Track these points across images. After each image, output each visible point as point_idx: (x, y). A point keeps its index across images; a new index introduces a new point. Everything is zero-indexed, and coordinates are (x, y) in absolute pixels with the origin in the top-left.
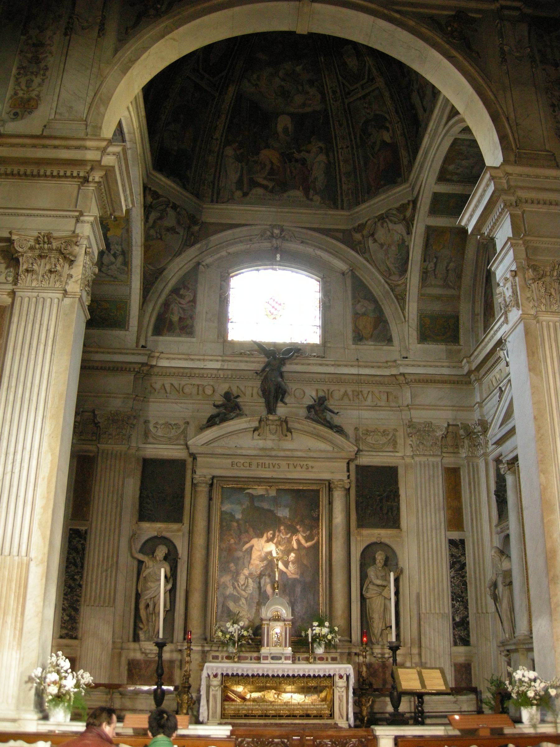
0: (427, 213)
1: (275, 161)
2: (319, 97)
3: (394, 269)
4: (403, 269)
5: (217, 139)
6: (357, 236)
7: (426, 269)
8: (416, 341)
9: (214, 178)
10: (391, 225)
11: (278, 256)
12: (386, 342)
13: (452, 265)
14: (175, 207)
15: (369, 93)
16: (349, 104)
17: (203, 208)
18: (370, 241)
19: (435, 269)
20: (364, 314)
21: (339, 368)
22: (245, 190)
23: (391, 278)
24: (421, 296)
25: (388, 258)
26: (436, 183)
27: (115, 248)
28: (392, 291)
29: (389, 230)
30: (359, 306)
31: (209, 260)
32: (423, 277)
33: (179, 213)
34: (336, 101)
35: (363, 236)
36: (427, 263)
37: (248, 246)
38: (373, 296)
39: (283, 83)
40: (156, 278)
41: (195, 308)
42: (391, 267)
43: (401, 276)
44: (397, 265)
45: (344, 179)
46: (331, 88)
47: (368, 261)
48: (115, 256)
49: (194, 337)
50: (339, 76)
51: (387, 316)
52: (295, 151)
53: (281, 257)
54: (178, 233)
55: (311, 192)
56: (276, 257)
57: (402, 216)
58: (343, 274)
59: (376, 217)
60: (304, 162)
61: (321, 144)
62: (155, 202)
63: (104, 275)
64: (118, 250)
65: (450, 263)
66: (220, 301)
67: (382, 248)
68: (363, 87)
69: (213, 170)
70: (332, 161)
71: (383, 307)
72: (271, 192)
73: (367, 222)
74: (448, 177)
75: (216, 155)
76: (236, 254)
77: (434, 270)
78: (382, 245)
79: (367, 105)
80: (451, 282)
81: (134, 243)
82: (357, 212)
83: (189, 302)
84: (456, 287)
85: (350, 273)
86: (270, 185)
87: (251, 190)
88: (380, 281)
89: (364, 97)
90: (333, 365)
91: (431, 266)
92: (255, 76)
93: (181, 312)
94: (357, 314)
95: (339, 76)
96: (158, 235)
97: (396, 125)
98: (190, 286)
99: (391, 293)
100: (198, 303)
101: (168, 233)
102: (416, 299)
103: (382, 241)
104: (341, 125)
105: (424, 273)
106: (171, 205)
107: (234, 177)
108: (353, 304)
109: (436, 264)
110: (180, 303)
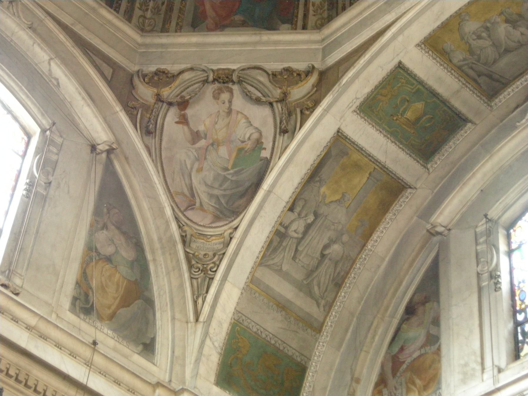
0: (358, 103)
3: (205, 198)
8: (213, 378)
12: (140, 348)
13: (336, 248)
18: (172, 115)
19: (302, 238)
20: (108, 259)
21: (41, 343)
23: (189, 213)
24: (252, 281)
25: (200, 170)
26: (418, 45)
28: (184, 242)
29: (229, 112)
30: (102, 236)
32: (271, 242)
35: (159, 98)
36: (292, 216)
43: (217, 218)
44: (216, 192)
57: (277, 93)
58: (93, 148)
59: (213, 70)
65: (335, 242)
67: (194, 142)
73: (181, 72)
74: (448, 45)
77: (299, 241)
78: (196, 136)
80: (319, 285)
84: (323, 302)
88: (161, 210)
90: (29, 328)
91: (298, 226)
99: (180, 247)
102: (242, 285)
103: (201, 128)
105: (277, 233)
109: (308, 227)
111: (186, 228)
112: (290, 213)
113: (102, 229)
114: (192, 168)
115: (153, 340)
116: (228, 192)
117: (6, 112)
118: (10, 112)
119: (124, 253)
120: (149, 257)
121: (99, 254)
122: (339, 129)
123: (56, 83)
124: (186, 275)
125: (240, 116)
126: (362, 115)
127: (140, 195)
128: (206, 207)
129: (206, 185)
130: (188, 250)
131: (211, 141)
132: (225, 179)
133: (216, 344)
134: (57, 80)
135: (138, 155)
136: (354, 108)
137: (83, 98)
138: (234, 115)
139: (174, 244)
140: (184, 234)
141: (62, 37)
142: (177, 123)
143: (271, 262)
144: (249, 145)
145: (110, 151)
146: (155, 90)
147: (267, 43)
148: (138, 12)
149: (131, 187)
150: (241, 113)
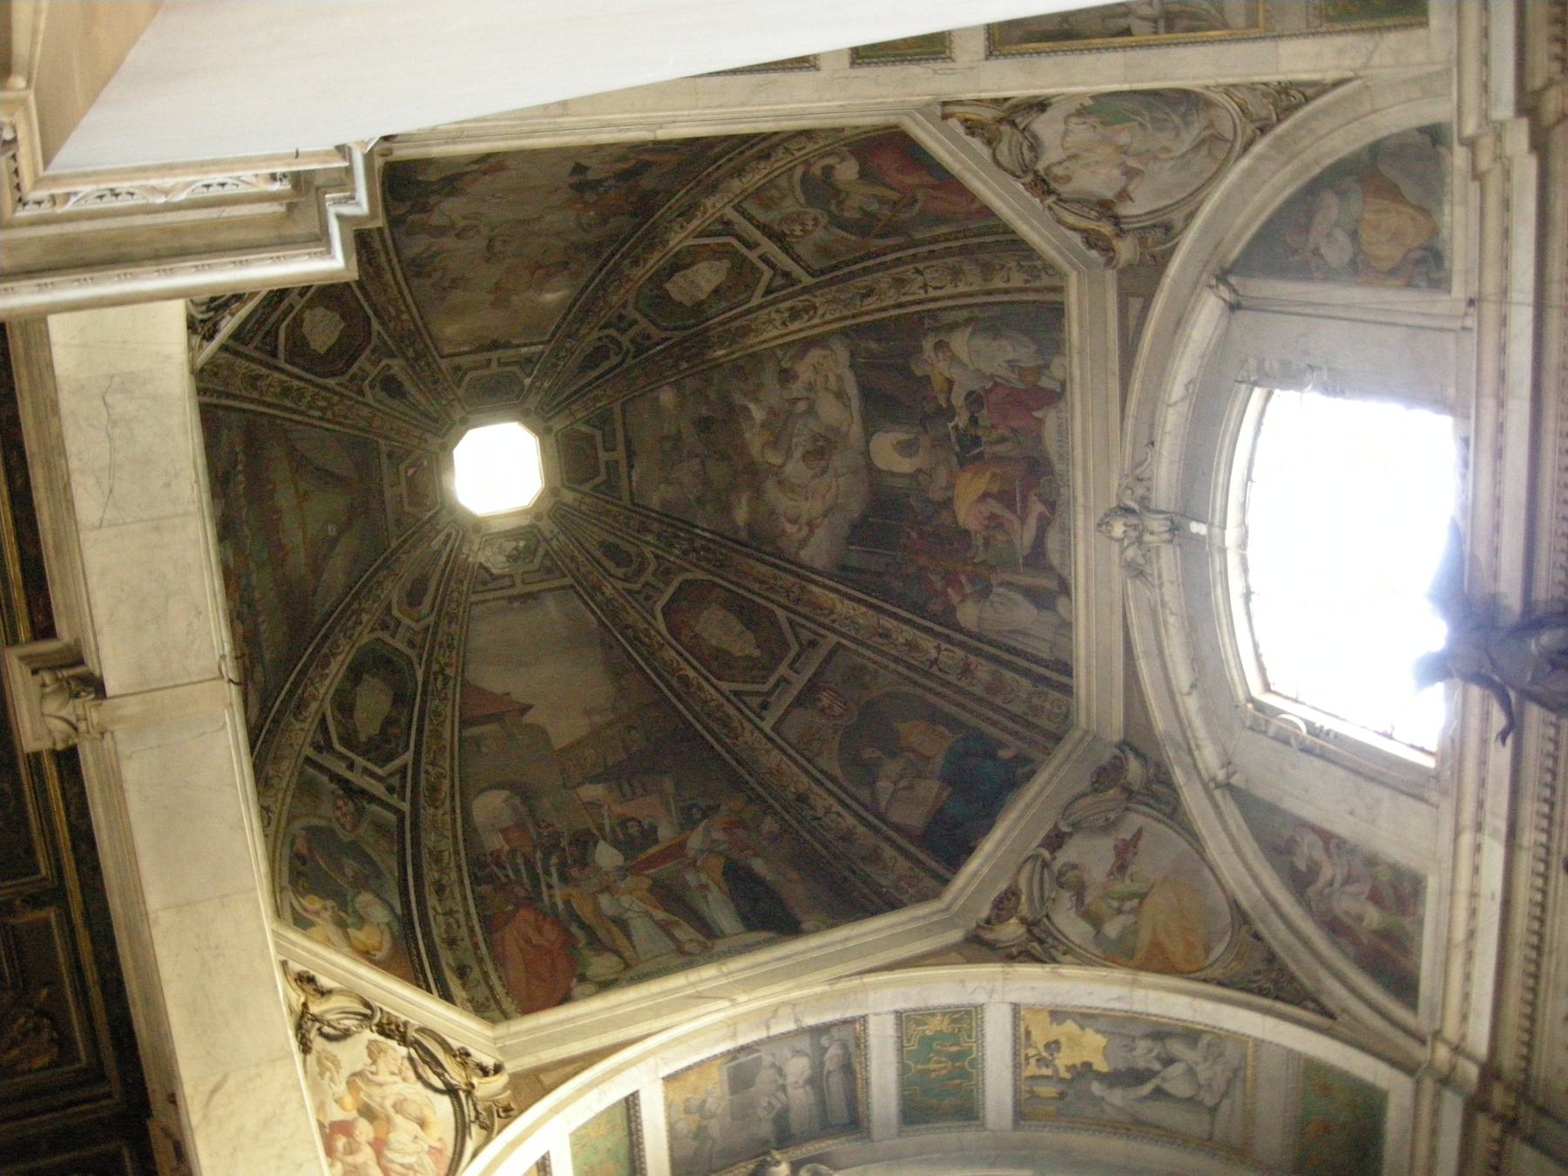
0: (939, 65)
1: (981, 484)
2: (815, 355)
4: (1184, 101)
5: (938, 648)
6: (1126, 249)
7: (1155, 21)
9: (1026, 673)
10: (1052, 155)
11: (1197, 528)
12: (1442, 150)
14: (1055, 841)
15: (757, 227)
16: (813, 275)
17: (1086, 732)
20: (1354, 236)
22: (1048, 583)
23: (1229, 135)
25: (1168, 150)
27: (1143, 1054)
29: (1074, 157)
31: (1209, 757)
33: (1076, 826)
34: (815, 308)
35: (1121, 233)
36: (1136, 25)
37: (1171, 620)
38: (1290, 203)
39: (798, 454)
40: (1257, 936)
41: (1345, 842)
42: (1189, 137)
43: (1209, 104)
44: (1177, 119)
45: (998, 283)
46: (784, 324)
47: (1190, 217)
48: (1169, 1061)
49: (1426, 877)
50: (754, 302)
51: (1357, 146)
52: (951, 425)
53: (1198, 521)
54: (1138, 835)
55: (1045, 382)
56: (1197, 534)
58: (1234, 307)
60: (974, 399)
61: (928, 344)
62: (1024, 909)
63: (1226, 1104)
64: (1150, 1051)
66: (1323, 755)
68: (750, 246)
69: (1008, 675)
70: (965, 314)
71: (1328, 161)
72: (1052, 506)
73: (1074, 229)
75: (972, 658)
76: (1196, 661)
78: (1130, 174)
79: (798, 229)
81: (1125, 1007)
82: (1061, 253)
83: (1327, 849)
85: (1233, 280)
86: (1037, 508)
87: (1052, 568)
88: (1249, 173)
89: (779, 238)
92: (790, 528)
93: (1350, 889)
94: (1353, 263)
95: (754, 302)
96: (1128, 905)
97: (798, 154)
98: (1287, 834)
99: (1280, 129)
100: (1327, 826)
101: (1132, 869)
103: (1116, 173)
104: (870, 292)
105: (1170, 28)
106: (1046, 854)
107: (1024, 614)
108: (1326, 279)
110: (1331, 884)
111: (1249, 132)
112: (1134, 29)
113: (1321, 256)
114: (1172, 159)
115: (1423, 130)
116: (1168, 110)
117: (1263, 428)
118: (1260, 422)
119: (1334, 214)
120: (1316, 170)
121: (1355, 255)
122: (987, 59)
123: (1191, 386)
124: (1308, 108)
125: (1067, 145)
126: (947, 43)
127: (1250, 209)
128: (1205, 123)
129: (1177, 135)
130: (1274, 118)
131: (1122, 156)
132: (1153, 120)
133: (1371, 45)
134: (1187, 387)
135: (1204, 231)
136: (951, 65)
137: (1185, 347)
138: (1069, 152)
139: (1280, 138)
140: (1258, 132)
141: (1136, 386)
142: (1131, 199)
143: (1213, 12)
144: (1092, 120)
145: (1222, 276)
146: (1114, 242)
147: (961, 162)
148: (1046, 281)
149: (1246, 226)
150: (1062, 145)
